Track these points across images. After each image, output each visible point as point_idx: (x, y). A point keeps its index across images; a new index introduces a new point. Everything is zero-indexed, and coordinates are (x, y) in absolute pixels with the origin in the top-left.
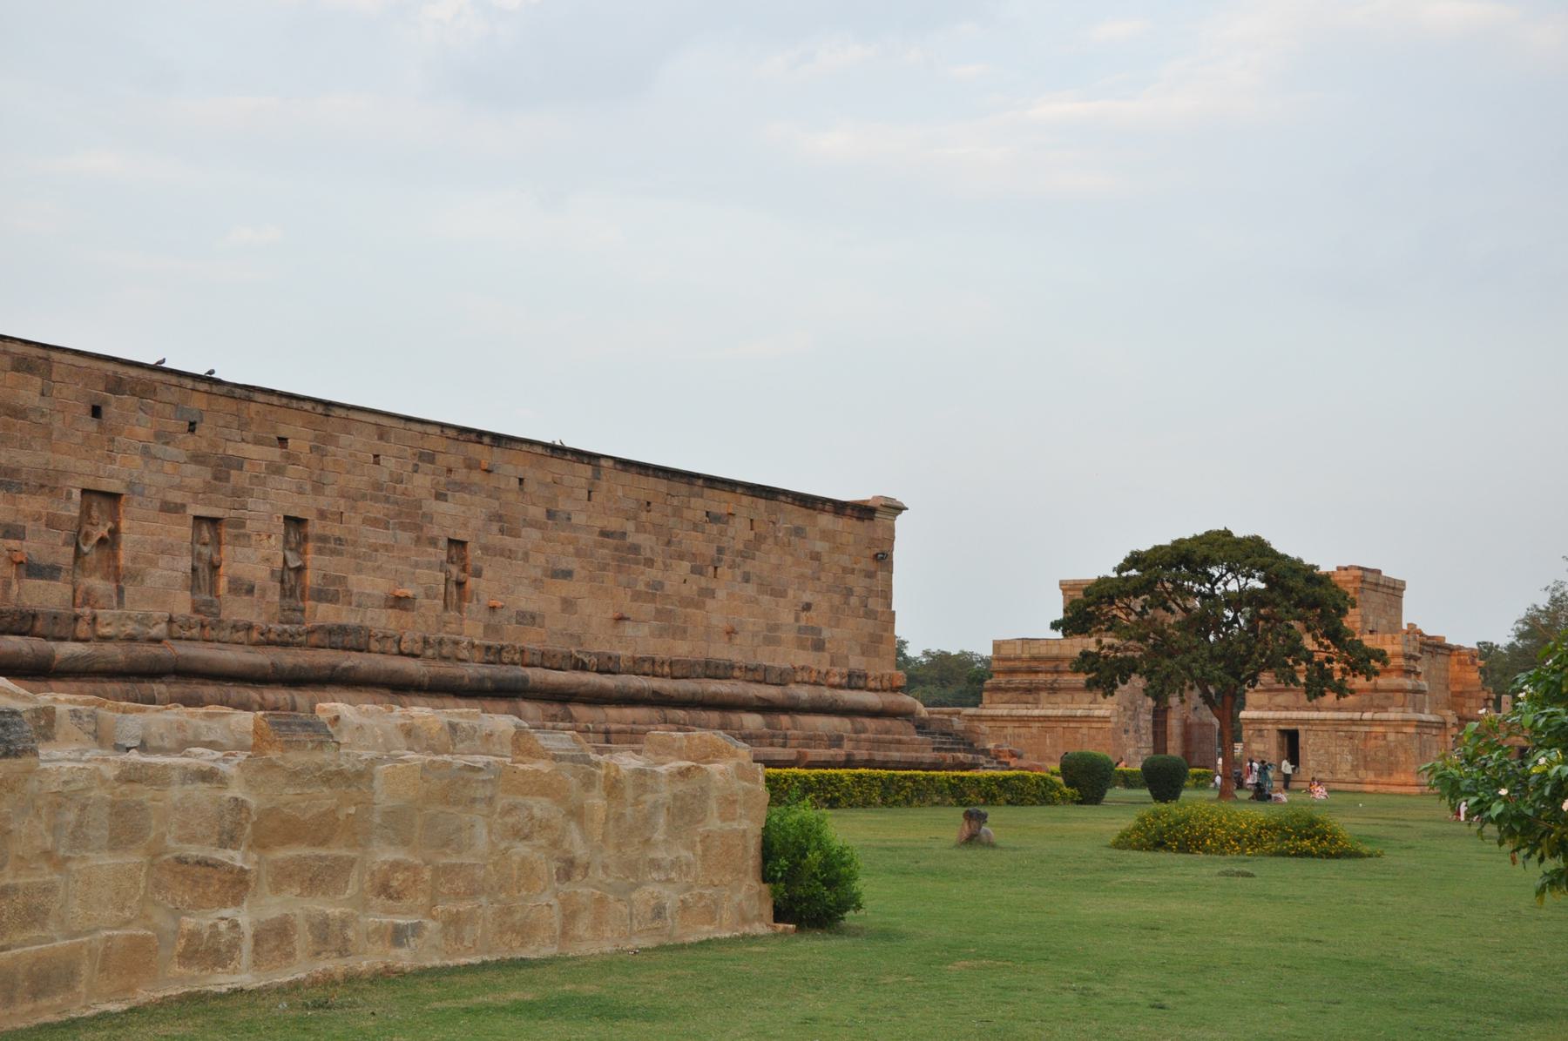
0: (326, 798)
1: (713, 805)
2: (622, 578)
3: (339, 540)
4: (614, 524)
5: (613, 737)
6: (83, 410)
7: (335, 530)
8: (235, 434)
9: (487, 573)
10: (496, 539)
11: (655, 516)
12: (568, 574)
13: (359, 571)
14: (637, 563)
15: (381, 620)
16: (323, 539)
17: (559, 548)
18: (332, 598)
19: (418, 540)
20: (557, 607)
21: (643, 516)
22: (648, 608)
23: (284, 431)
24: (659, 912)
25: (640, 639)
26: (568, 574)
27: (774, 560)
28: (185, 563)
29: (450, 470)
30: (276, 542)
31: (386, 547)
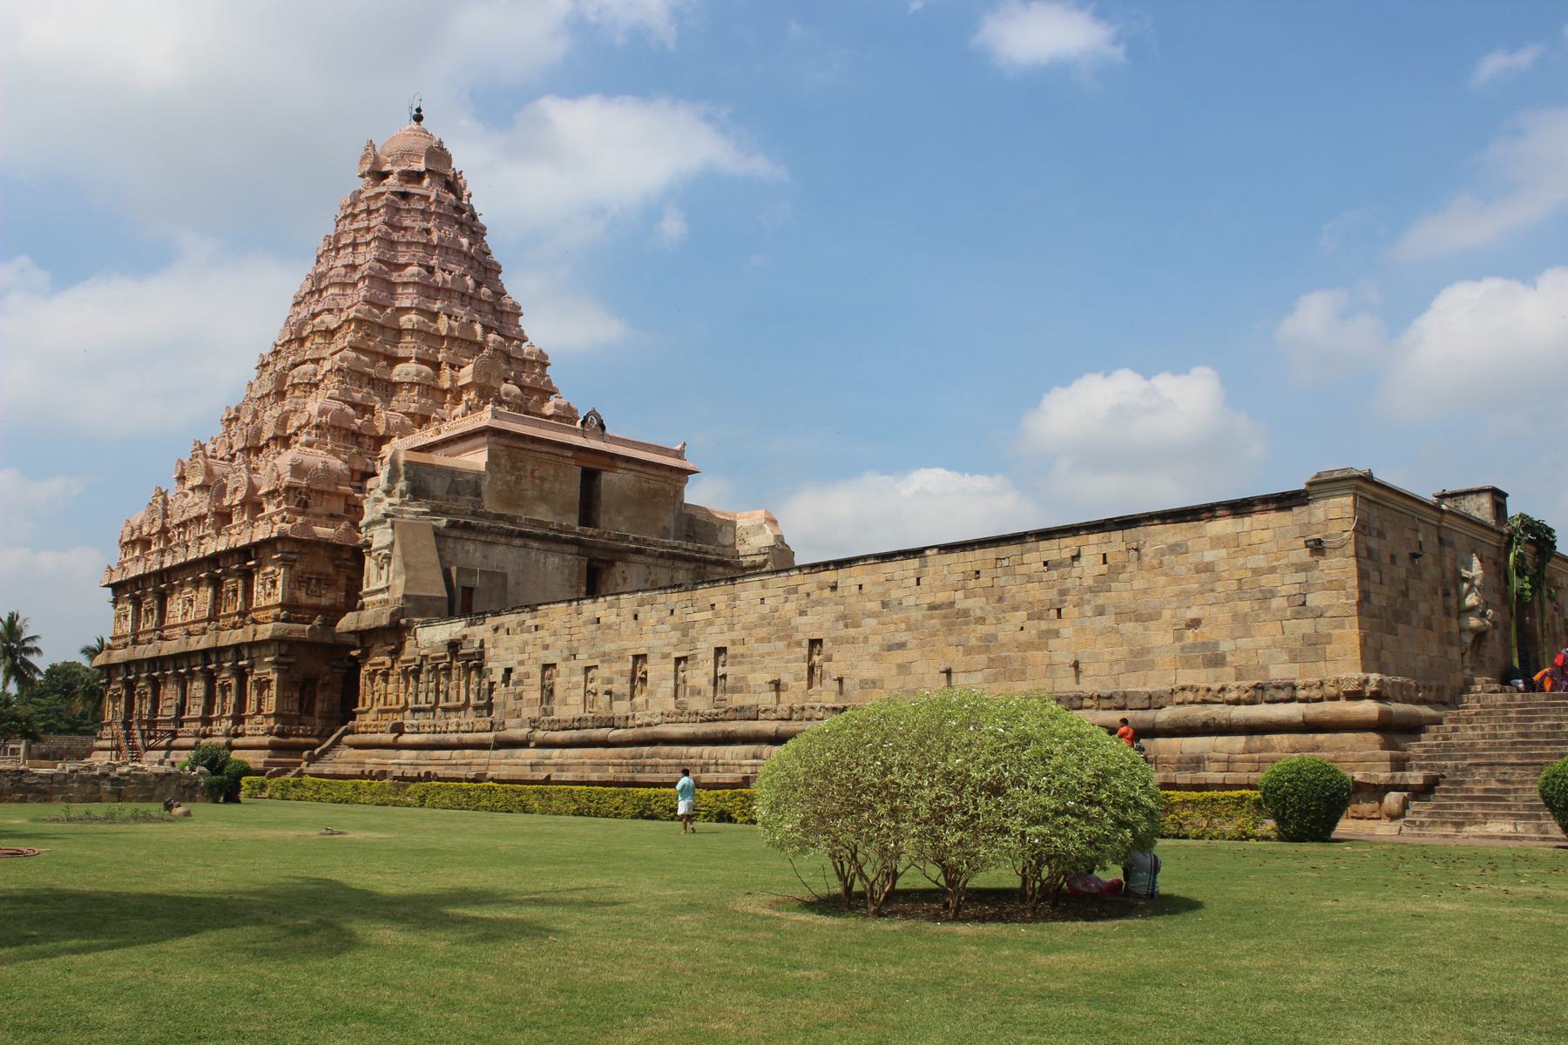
2: (953, 639)
4: (941, 597)
6: (631, 617)
7: (740, 649)
8: (690, 610)
9: (836, 657)
11: (985, 580)
13: (753, 671)
14: (967, 624)
15: (767, 699)
16: (734, 657)
17: (892, 627)
18: (740, 690)
19: (789, 645)
20: (894, 671)
21: (972, 584)
22: (981, 659)
27: (1137, 585)
28: (671, 683)
30: (711, 663)
31: (769, 654)
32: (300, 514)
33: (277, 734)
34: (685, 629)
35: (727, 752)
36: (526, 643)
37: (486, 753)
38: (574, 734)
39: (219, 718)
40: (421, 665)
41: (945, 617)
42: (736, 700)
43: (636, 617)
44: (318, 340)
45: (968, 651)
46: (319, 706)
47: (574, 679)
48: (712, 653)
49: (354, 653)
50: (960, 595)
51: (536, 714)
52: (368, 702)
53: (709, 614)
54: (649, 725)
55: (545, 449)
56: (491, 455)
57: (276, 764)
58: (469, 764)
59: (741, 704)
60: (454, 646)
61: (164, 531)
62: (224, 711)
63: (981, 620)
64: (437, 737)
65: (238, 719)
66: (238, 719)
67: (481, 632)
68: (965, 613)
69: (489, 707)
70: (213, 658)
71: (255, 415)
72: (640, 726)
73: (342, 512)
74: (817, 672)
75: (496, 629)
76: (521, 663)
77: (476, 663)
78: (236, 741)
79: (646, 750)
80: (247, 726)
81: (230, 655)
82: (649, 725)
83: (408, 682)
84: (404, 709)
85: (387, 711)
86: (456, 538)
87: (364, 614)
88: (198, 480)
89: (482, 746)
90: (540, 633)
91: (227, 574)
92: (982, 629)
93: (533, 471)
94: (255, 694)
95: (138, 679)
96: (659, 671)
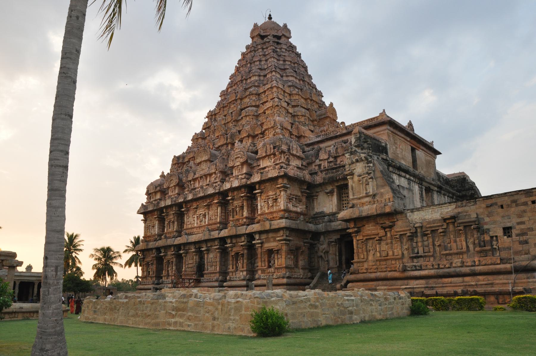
0: (183, 305)
1: (243, 309)
24: (229, 328)
33: (288, 278)
36: (524, 211)
37: (501, 277)
44: (254, 98)
46: (301, 263)
55: (403, 136)
58: (492, 284)
73: (300, 166)
81: (243, 239)
83: (402, 243)
85: (386, 260)
88: (205, 158)
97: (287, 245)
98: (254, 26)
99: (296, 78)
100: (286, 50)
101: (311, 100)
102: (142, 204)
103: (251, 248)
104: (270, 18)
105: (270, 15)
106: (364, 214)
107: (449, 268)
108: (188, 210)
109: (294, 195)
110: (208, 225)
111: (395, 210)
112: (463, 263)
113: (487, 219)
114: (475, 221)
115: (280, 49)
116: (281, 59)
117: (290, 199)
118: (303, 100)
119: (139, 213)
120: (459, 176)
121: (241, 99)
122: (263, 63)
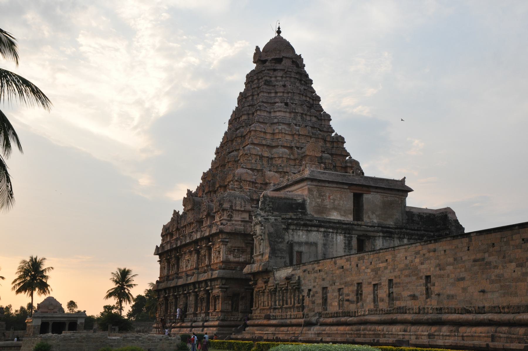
2: (484, 276)
3: (399, 283)
4: (479, 256)
5: (465, 338)
6: (355, 265)
7: (398, 280)
8: (378, 262)
9: (436, 284)
10: (438, 272)
11: (497, 248)
12: (463, 279)
13: (404, 290)
14: (490, 268)
15: (410, 303)
16: (396, 284)
19: (417, 279)
21: (491, 249)
23: (387, 258)
25: (495, 298)
26: (463, 279)
28: (372, 296)
29: (424, 255)
30: (387, 287)
31: (410, 282)
32: (229, 221)
33: (222, 320)
34: (376, 271)
35: (395, 329)
36: (316, 278)
38: (335, 320)
39: (200, 313)
40: (276, 288)
41: (480, 265)
42: (398, 304)
43: (357, 265)
44: (239, 141)
45: (492, 282)
46: (240, 307)
47: (335, 294)
48: (387, 283)
49: (251, 283)
50: (486, 255)
51: (320, 310)
52: (257, 305)
53: (384, 264)
54: (364, 315)
55: (335, 186)
56: (310, 190)
57: (222, 334)
58: (294, 333)
59: (399, 305)
60: (288, 279)
61: (178, 229)
62: (202, 310)
63: (496, 267)
64: (283, 321)
65: (207, 314)
66: (207, 314)
67: (299, 272)
68: (489, 263)
69: (303, 308)
70: (197, 286)
71: (214, 176)
72: (360, 316)
74: (430, 291)
75: (304, 271)
76: (314, 287)
77: (298, 287)
78: (205, 324)
79: (362, 327)
80: (210, 317)
82: (364, 315)
84: (270, 309)
85: (264, 309)
86: (293, 230)
87: (255, 266)
89: (298, 325)
90: (322, 273)
91: (201, 248)
92: (497, 271)
93: (329, 197)
94: (213, 301)
95: (169, 296)
96: (367, 290)
97: (225, 292)
98: (256, 50)
99: (284, 111)
100: (282, 77)
101: (299, 135)
102: (157, 246)
103: (207, 292)
104: (279, 32)
105: (279, 28)
106: (253, 271)
107: (286, 319)
108: (182, 255)
109: (235, 247)
110: (190, 270)
111: (267, 269)
112: (291, 315)
113: (303, 282)
114: (295, 283)
115: (276, 77)
116: (273, 91)
117: (230, 251)
118: (289, 138)
119: (155, 254)
120: (443, 213)
121: (232, 141)
122: (255, 97)
